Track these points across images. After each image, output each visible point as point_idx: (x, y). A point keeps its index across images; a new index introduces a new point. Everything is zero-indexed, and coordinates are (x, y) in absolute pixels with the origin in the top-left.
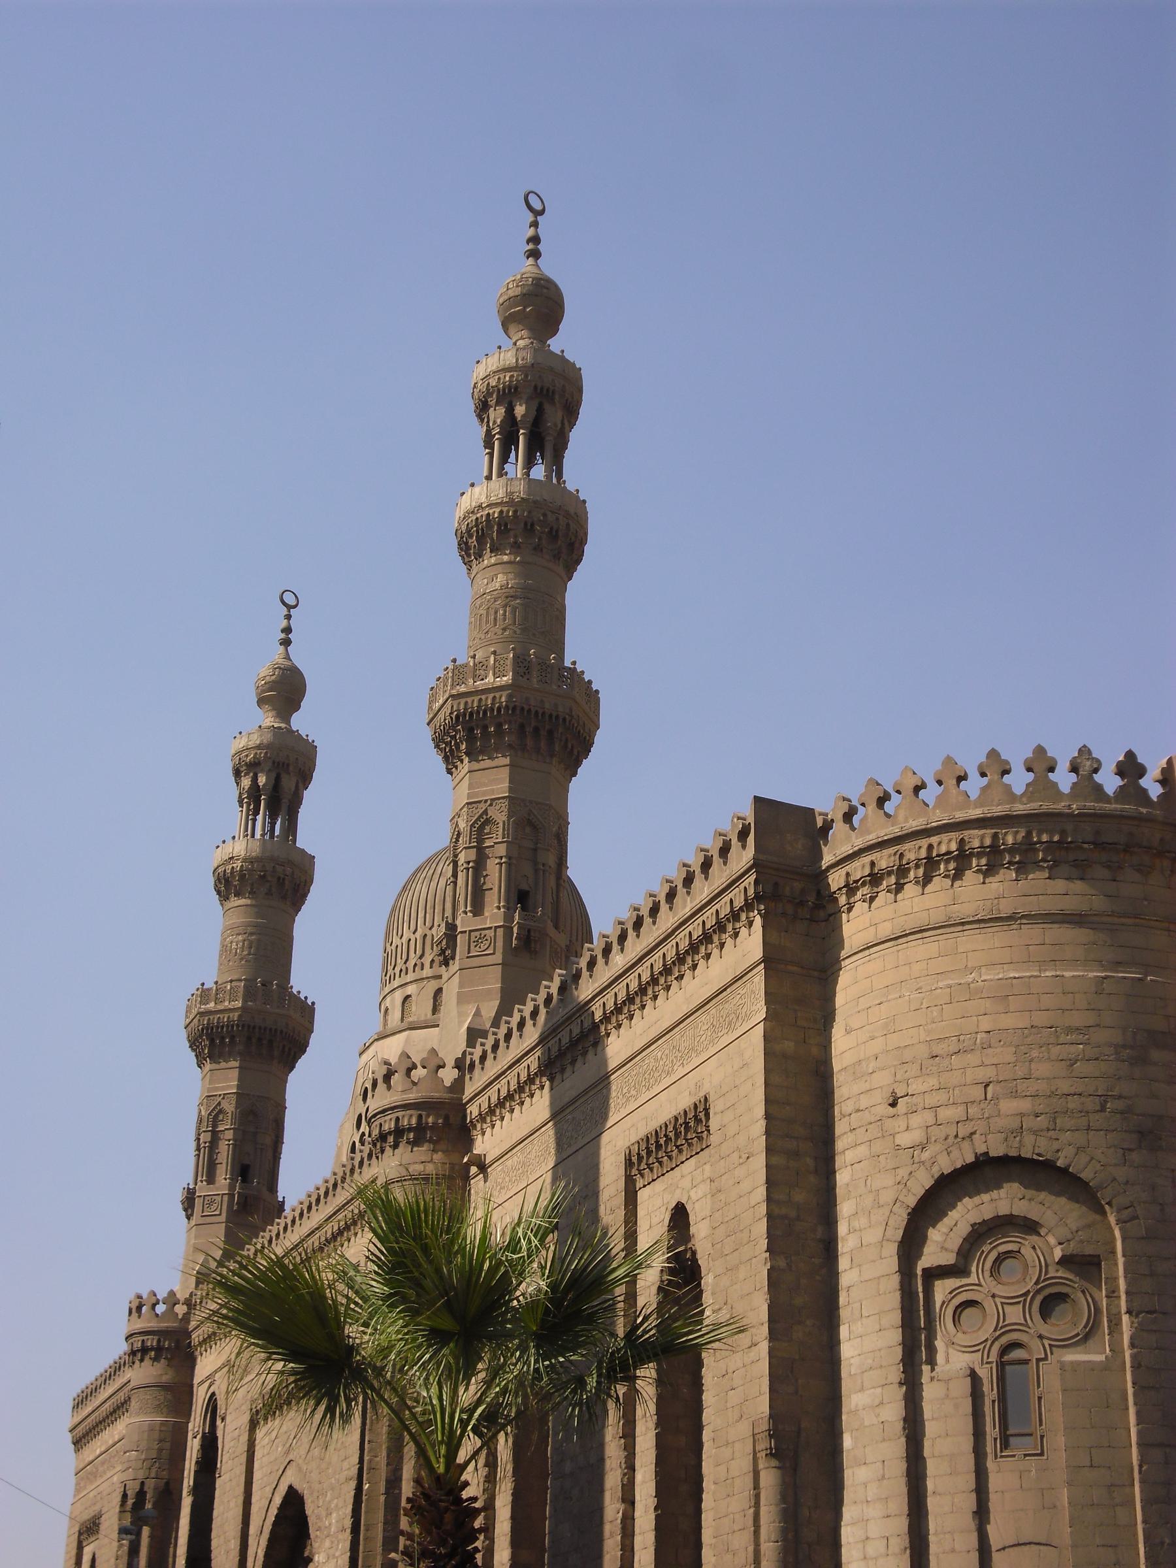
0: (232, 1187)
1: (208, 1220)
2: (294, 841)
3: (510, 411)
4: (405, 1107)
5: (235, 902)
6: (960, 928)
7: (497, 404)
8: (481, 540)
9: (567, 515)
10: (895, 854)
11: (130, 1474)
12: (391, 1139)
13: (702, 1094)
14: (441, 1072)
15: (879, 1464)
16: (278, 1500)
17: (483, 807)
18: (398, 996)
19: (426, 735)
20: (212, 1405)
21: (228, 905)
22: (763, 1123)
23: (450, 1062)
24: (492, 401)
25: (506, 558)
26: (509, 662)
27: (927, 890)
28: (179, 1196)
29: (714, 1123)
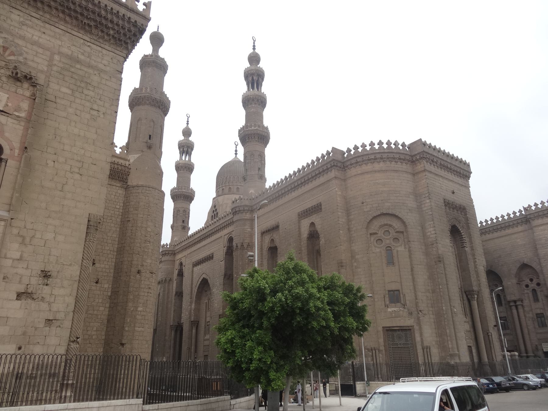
11: (163, 277)
16: (200, 280)
18: (221, 189)
20: (181, 264)
29: (323, 207)
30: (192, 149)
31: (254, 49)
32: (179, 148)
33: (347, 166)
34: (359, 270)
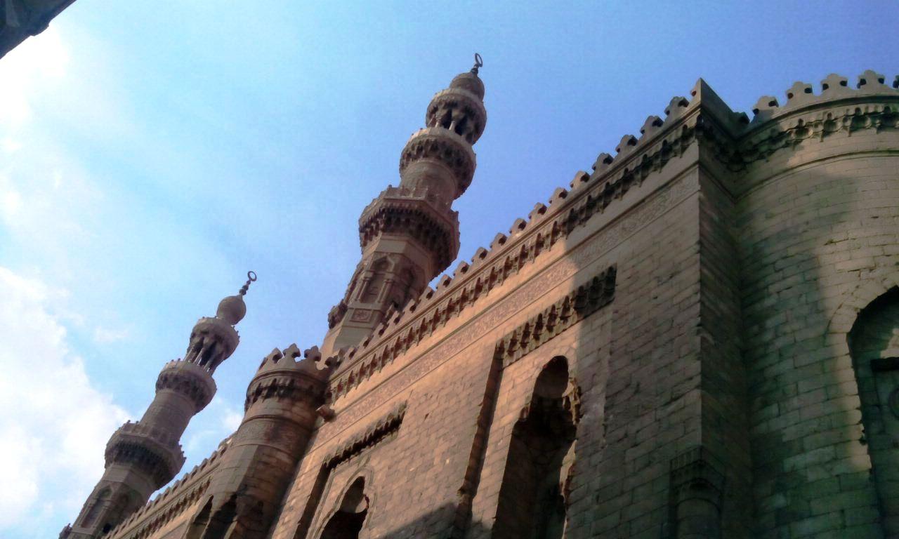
3: (449, 114)
4: (283, 373)
5: (166, 391)
6: (887, 154)
7: (444, 108)
8: (420, 150)
9: (469, 159)
10: (824, 113)
12: (265, 393)
13: (605, 269)
14: (316, 362)
17: (385, 255)
19: (356, 226)
21: (162, 391)
22: (697, 247)
23: (324, 359)
24: (440, 108)
25: (431, 161)
26: (425, 192)
27: (854, 134)
31: (475, 71)
32: (193, 336)
33: (755, 149)
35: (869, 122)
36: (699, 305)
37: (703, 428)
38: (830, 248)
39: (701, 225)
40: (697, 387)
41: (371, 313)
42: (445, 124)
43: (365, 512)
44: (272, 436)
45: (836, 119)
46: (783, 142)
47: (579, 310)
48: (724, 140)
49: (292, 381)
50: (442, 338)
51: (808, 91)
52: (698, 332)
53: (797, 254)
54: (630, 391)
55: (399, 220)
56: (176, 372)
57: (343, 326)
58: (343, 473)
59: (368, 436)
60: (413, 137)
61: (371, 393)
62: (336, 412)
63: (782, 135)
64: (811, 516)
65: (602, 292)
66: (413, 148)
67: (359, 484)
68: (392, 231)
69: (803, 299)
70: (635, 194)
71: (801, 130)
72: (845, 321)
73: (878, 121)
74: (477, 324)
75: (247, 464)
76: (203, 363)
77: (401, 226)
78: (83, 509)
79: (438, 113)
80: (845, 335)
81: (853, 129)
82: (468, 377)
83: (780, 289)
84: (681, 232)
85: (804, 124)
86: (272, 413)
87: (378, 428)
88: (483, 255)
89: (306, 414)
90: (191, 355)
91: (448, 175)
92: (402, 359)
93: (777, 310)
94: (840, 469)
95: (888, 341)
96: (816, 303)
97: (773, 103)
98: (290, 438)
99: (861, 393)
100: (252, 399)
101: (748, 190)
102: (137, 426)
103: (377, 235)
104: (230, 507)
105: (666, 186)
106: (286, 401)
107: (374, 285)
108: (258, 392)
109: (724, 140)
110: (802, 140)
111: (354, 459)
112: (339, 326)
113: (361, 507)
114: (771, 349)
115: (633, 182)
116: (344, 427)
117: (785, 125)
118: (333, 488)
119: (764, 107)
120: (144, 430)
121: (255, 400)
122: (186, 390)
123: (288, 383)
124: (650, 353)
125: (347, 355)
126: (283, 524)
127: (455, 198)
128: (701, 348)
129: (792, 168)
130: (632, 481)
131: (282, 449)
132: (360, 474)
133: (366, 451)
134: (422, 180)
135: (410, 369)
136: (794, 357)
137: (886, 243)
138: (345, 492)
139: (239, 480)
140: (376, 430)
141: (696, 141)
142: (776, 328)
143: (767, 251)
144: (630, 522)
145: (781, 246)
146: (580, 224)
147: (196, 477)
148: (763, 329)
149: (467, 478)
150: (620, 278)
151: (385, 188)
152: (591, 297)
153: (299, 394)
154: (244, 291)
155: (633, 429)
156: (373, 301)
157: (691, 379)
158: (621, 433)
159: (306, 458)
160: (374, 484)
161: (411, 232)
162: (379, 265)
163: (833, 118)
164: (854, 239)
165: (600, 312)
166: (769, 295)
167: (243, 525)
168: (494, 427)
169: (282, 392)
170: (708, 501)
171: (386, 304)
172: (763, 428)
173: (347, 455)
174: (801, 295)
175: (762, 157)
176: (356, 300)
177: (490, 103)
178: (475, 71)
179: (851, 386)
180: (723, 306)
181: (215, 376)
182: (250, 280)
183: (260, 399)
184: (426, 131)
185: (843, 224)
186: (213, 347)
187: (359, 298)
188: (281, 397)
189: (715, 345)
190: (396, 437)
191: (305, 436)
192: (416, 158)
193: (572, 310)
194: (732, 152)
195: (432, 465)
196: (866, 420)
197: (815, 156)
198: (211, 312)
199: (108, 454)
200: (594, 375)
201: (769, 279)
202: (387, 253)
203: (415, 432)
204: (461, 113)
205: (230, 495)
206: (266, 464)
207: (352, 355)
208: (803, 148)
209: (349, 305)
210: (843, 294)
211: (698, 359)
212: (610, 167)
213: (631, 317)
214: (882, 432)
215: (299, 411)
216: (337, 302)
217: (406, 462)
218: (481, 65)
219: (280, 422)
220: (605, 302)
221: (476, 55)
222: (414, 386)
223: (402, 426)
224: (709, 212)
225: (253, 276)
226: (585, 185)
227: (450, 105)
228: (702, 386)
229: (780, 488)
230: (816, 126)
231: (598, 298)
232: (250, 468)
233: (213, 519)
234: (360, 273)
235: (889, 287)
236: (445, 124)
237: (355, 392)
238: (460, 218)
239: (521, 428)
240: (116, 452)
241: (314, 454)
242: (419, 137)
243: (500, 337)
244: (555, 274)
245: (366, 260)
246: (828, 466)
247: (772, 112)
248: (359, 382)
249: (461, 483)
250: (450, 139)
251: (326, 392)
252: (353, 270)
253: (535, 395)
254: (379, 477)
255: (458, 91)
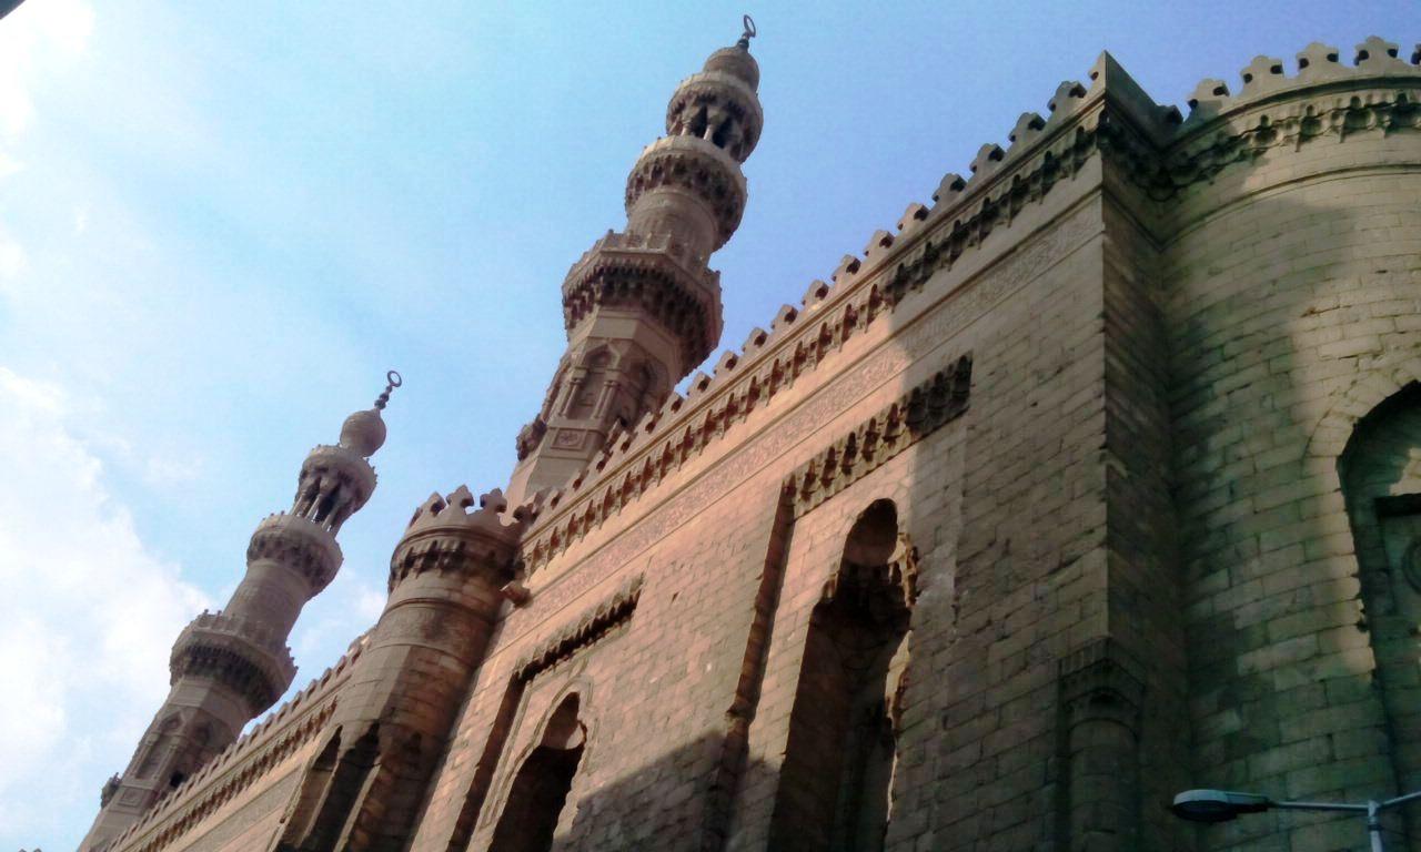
0: (159, 787)
1: (125, 809)
2: (334, 533)
3: (703, 113)
4: (448, 531)
5: (263, 562)
7: (695, 104)
8: (657, 173)
9: (736, 185)
10: (1302, 106)
12: (419, 563)
13: (956, 357)
14: (499, 514)
15: (1322, 742)
17: (604, 342)
21: (256, 563)
22: (1100, 323)
23: (511, 509)
25: (675, 191)
27: (1349, 139)
28: (103, 782)
30: (360, 497)
31: (744, 44)
32: (304, 475)
34: (1274, 760)
35: (1372, 119)
36: (1103, 415)
37: (1111, 608)
38: (1309, 322)
39: (1106, 288)
40: (1101, 545)
41: (584, 434)
42: (697, 130)
43: (580, 748)
44: (433, 631)
45: (1321, 114)
46: (1237, 153)
47: (913, 426)
48: (1142, 151)
49: (462, 545)
50: (697, 472)
51: (1277, 70)
52: (1102, 459)
53: (1259, 331)
54: (994, 553)
55: (625, 286)
56: (277, 533)
57: (541, 456)
58: (546, 688)
59: (583, 629)
60: (646, 152)
61: (586, 562)
62: (532, 592)
63: (1235, 141)
64: (1280, 745)
65: (949, 396)
66: (646, 169)
67: (571, 704)
68: (616, 304)
69: (1268, 403)
70: (1000, 238)
71: (1265, 132)
72: (1334, 437)
73: (1387, 118)
74: (752, 451)
75: (394, 675)
76: (320, 518)
77: (630, 296)
78: (139, 750)
79: (685, 113)
80: (1334, 461)
81: (1348, 131)
82: (741, 533)
83: (1230, 387)
84: (1075, 299)
85: (1270, 123)
86: (432, 594)
87: (599, 617)
88: (761, 340)
89: (486, 597)
90: (301, 505)
91: (702, 213)
92: (635, 507)
93: (1225, 421)
94: (1325, 670)
95: (1400, 468)
96: (1288, 409)
97: (1220, 91)
98: (461, 635)
99: (1359, 551)
100: (399, 573)
101: (1178, 230)
102: (218, 620)
103: (591, 310)
104: (368, 743)
105: (1051, 225)
106: (454, 575)
107: (588, 390)
108: (409, 562)
109: (1142, 151)
110: (1267, 148)
111: (562, 665)
112: (533, 457)
113: (574, 741)
114: (1217, 483)
115: (999, 220)
116: (546, 616)
117: (1240, 126)
118: (529, 711)
119: (1207, 97)
120: (231, 624)
121: (404, 576)
122: (295, 561)
123: (455, 547)
124: (1024, 493)
125: (547, 502)
126: (453, 768)
127: (715, 249)
128: (1108, 482)
129: (1251, 195)
130: (997, 696)
131: (449, 651)
132: (572, 689)
133: (580, 652)
134: (661, 222)
135: (647, 523)
136: (1252, 495)
137: (1399, 312)
138: (549, 716)
139: (382, 701)
140: (596, 620)
141: (1098, 152)
142: (1225, 449)
143: (1212, 327)
144: (996, 756)
145: (1231, 320)
146: (913, 288)
147: (314, 697)
148: (1204, 452)
149: (740, 692)
150: (978, 374)
151: (601, 234)
152: (933, 405)
153: (472, 561)
154: (382, 401)
155: (998, 612)
156: (588, 416)
157: (1091, 531)
158: (980, 619)
159: (486, 666)
160: (595, 702)
161: (645, 305)
162: (596, 358)
163: (1315, 113)
164: (1349, 307)
165: (945, 430)
166: (1215, 398)
167: (390, 771)
168: (780, 613)
169: (446, 561)
170: (1119, 723)
171: (607, 421)
172: (1204, 607)
173: (551, 659)
174: (1264, 397)
175: (1202, 177)
176: (560, 414)
177: (769, 96)
178: (744, 44)
179: (1345, 541)
180: (1141, 418)
181: (338, 538)
182: (392, 385)
183: (412, 574)
184: (667, 141)
185: (1332, 283)
186: (335, 491)
187: (565, 412)
188: (446, 569)
189: (1129, 476)
190: (627, 629)
191: (486, 628)
192: (651, 185)
193: (902, 426)
194: (1154, 168)
195: (684, 674)
196: (1366, 593)
197: (1287, 174)
198: (329, 434)
199: (175, 662)
200: (937, 529)
201: (1212, 373)
202: (608, 339)
203: (657, 622)
204: (723, 114)
205: (370, 723)
206: (422, 674)
207: (555, 501)
208: (1267, 162)
209: (550, 422)
210: (1331, 394)
211: (1103, 500)
212: (961, 196)
213: (995, 435)
214: (1393, 611)
215: (474, 592)
216: (530, 419)
217: (646, 668)
218: (754, 35)
219: (444, 609)
220: (953, 414)
221: (746, 17)
222: (654, 550)
223: (637, 613)
224: (1118, 266)
225: (395, 379)
226: (923, 225)
227: (705, 100)
228: (1108, 543)
229: (1229, 702)
230: (1289, 126)
231: (943, 407)
232: (399, 682)
233: (342, 760)
234: (565, 371)
235: (1404, 382)
236: (697, 130)
237: (561, 560)
238: (723, 282)
239: (826, 615)
240: (188, 659)
241: (498, 659)
242: (655, 152)
243: (788, 471)
244: (876, 368)
245: (574, 350)
246: (1308, 666)
247: (1219, 104)
248: (568, 545)
249: (731, 700)
250: (705, 154)
251: (516, 560)
252: (552, 368)
253: (845, 561)
254: (602, 695)
255: (716, 76)
